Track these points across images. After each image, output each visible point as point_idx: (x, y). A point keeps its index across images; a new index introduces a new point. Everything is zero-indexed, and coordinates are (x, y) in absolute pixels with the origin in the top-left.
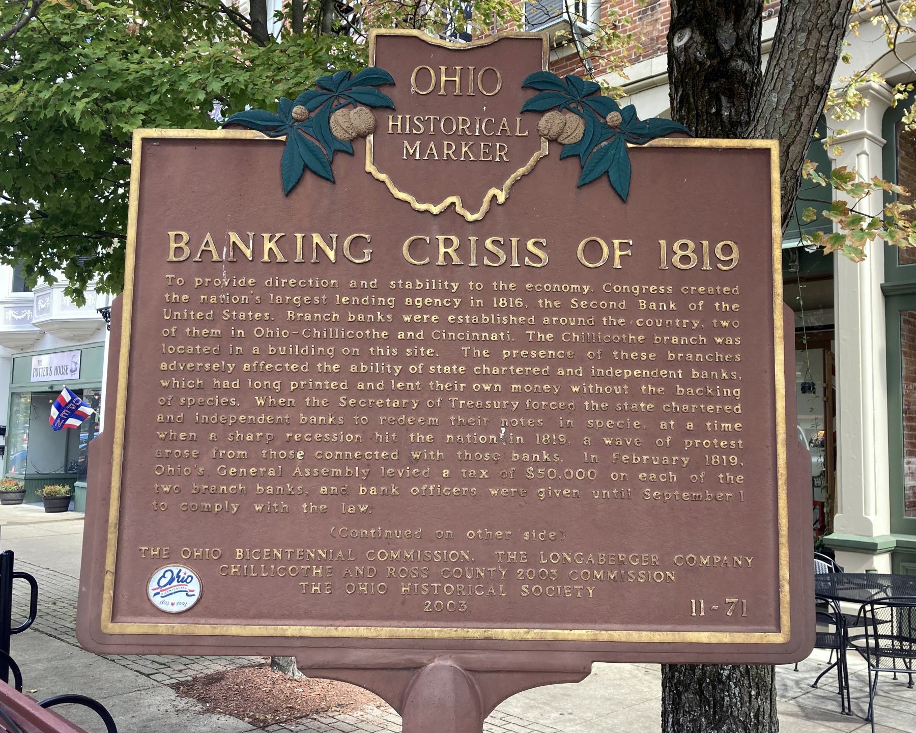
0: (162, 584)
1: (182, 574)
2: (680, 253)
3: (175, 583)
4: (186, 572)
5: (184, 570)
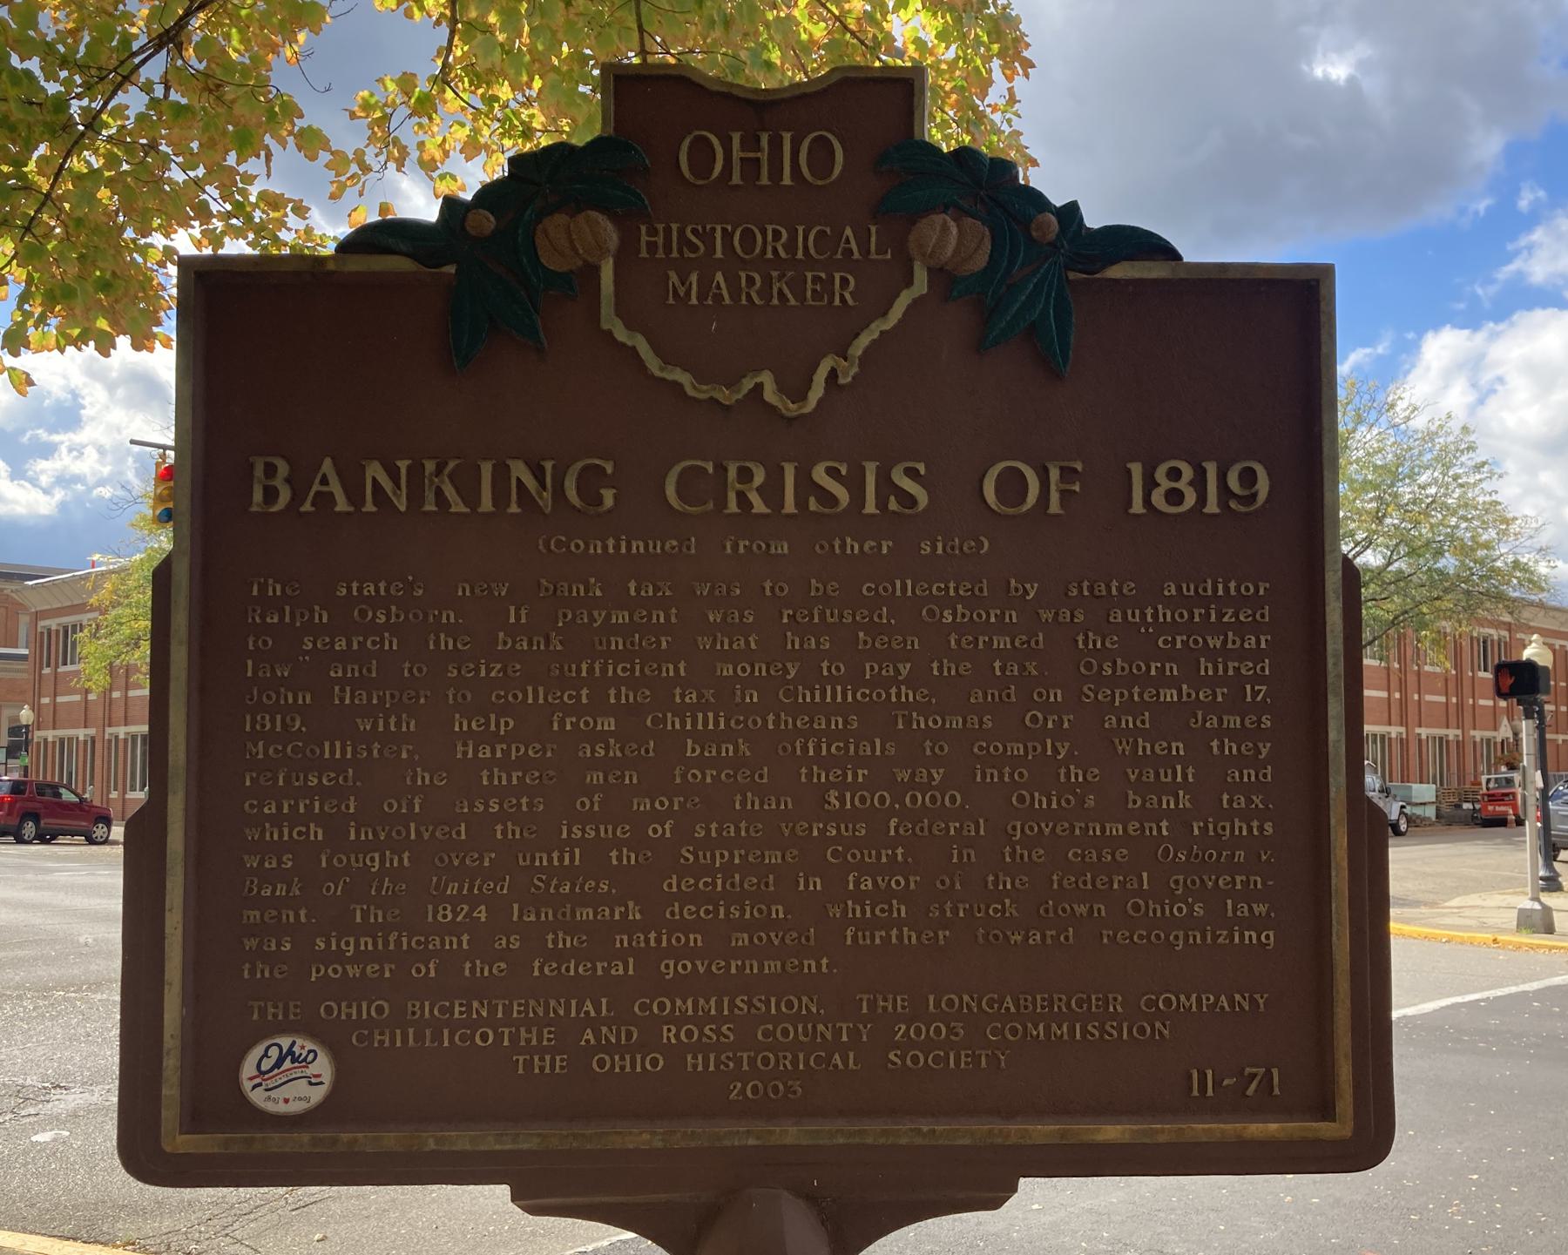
0: (263, 1068)
1: (296, 1049)
2: (1166, 484)
3: (287, 1064)
4: (303, 1045)
5: (299, 1042)
